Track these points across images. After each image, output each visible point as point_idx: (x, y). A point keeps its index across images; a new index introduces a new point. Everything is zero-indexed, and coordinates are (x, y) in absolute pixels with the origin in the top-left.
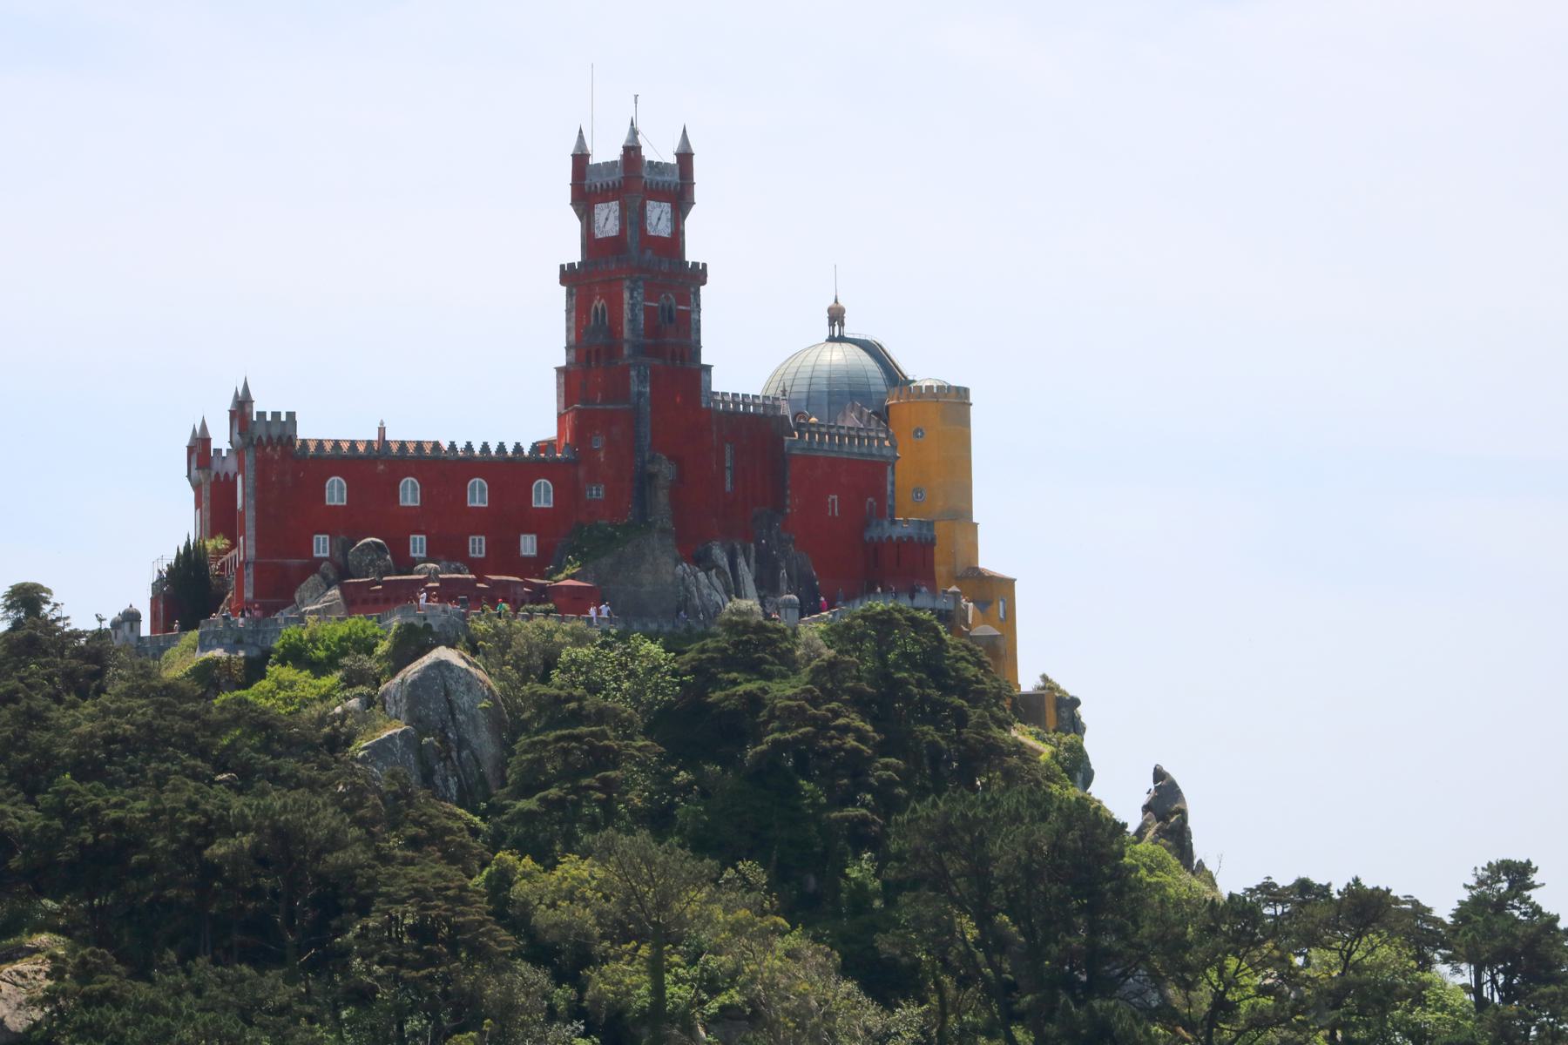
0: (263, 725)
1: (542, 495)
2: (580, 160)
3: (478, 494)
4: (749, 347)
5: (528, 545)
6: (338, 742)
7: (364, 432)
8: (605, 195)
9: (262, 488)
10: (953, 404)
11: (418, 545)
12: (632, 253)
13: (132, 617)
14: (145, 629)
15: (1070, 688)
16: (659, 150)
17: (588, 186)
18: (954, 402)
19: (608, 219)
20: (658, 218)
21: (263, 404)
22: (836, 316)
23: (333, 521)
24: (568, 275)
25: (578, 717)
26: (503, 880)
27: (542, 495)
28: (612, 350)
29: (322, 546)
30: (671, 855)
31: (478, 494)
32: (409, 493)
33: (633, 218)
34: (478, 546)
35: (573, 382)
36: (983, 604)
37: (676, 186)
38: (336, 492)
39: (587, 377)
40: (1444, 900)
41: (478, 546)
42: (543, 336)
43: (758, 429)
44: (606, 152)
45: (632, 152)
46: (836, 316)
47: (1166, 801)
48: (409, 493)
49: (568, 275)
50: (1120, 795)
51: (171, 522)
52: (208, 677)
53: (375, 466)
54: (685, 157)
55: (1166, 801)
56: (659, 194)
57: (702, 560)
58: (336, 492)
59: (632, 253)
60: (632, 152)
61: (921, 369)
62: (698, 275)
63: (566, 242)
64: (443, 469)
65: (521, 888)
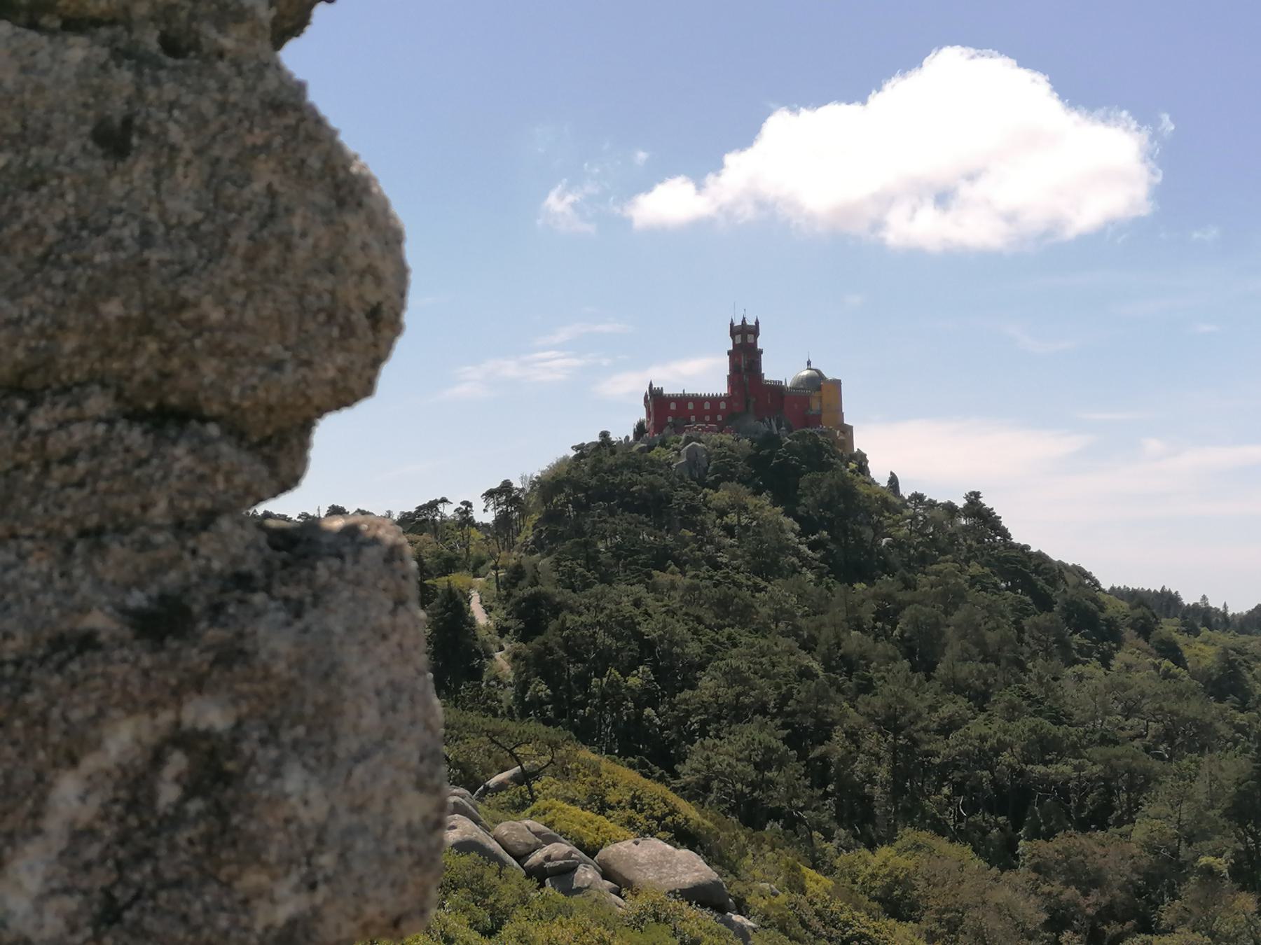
0: (652, 461)
1: (723, 406)
2: (732, 324)
3: (707, 406)
5: (720, 418)
6: (669, 465)
9: (655, 405)
10: (837, 384)
11: (693, 418)
12: (745, 348)
13: (627, 438)
15: (864, 451)
17: (734, 331)
18: (837, 384)
19: (739, 339)
20: (750, 338)
22: (809, 363)
23: (672, 413)
24: (729, 353)
25: (725, 457)
26: (705, 496)
27: (723, 406)
29: (670, 419)
30: (743, 490)
31: (707, 406)
32: (691, 406)
33: (744, 338)
34: (707, 418)
35: (732, 380)
36: (843, 432)
37: (755, 330)
38: (673, 406)
40: (960, 503)
41: (707, 418)
42: (723, 365)
43: (777, 390)
44: (738, 323)
45: (744, 321)
46: (809, 363)
47: (893, 480)
48: (691, 406)
51: (642, 414)
52: (641, 450)
53: (682, 400)
54: (757, 323)
55: (893, 480)
56: (750, 333)
57: (762, 420)
58: (673, 406)
59: (745, 348)
60: (744, 321)
61: (829, 375)
62: (761, 352)
64: (698, 400)
65: (709, 498)
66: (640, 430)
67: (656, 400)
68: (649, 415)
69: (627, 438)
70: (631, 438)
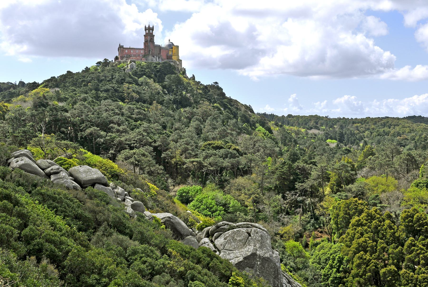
2: (145, 27)
7: (129, 47)
8: (147, 29)
10: (177, 47)
13: (112, 61)
14: (113, 61)
16: (151, 26)
18: (177, 47)
19: (147, 31)
20: (151, 31)
22: (169, 40)
28: (147, 41)
33: (149, 31)
35: (145, 44)
37: (153, 29)
39: (146, 42)
42: (143, 40)
43: (159, 47)
44: (147, 26)
45: (149, 26)
46: (169, 40)
49: (144, 36)
54: (153, 27)
57: (154, 57)
60: (149, 26)
61: (175, 44)
66: (116, 58)
69: (112, 61)
70: (113, 61)
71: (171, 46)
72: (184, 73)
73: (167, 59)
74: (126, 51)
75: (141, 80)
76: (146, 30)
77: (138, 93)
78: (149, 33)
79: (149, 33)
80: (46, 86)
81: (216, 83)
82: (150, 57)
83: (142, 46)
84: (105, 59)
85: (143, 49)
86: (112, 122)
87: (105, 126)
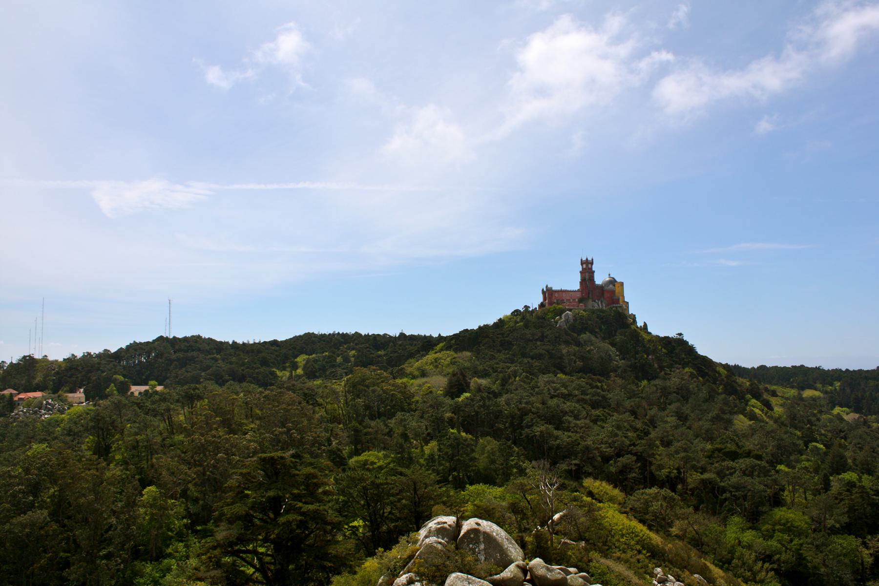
4: (600, 279)
10: (622, 284)
16: (590, 259)
17: (582, 263)
18: (622, 284)
19: (584, 266)
21: (549, 286)
33: (587, 266)
37: (592, 263)
42: (578, 278)
43: (601, 288)
44: (584, 259)
50: (640, 324)
51: (540, 299)
61: (618, 280)
63: (580, 268)
66: (542, 305)
67: (548, 293)
68: (545, 299)
71: (613, 282)
72: (635, 321)
73: (614, 303)
74: (556, 295)
75: (585, 336)
76: (582, 264)
77: (582, 358)
78: (587, 270)
79: (587, 270)
80: (448, 348)
81: (680, 334)
82: (590, 302)
83: (576, 286)
84: (526, 306)
85: (578, 291)
86: (565, 413)
87: (556, 420)
